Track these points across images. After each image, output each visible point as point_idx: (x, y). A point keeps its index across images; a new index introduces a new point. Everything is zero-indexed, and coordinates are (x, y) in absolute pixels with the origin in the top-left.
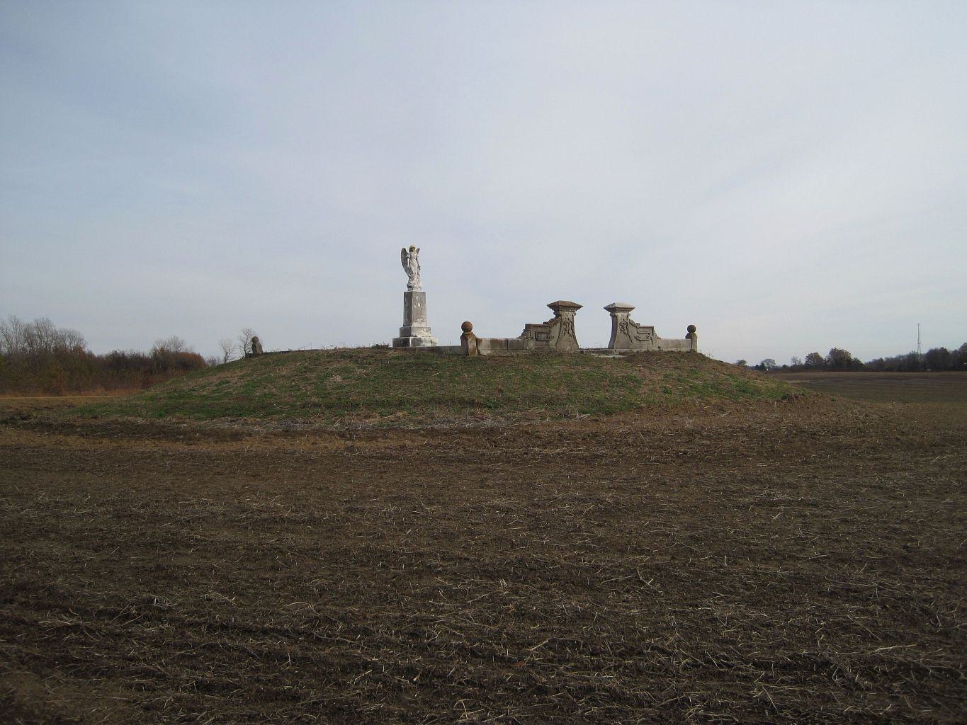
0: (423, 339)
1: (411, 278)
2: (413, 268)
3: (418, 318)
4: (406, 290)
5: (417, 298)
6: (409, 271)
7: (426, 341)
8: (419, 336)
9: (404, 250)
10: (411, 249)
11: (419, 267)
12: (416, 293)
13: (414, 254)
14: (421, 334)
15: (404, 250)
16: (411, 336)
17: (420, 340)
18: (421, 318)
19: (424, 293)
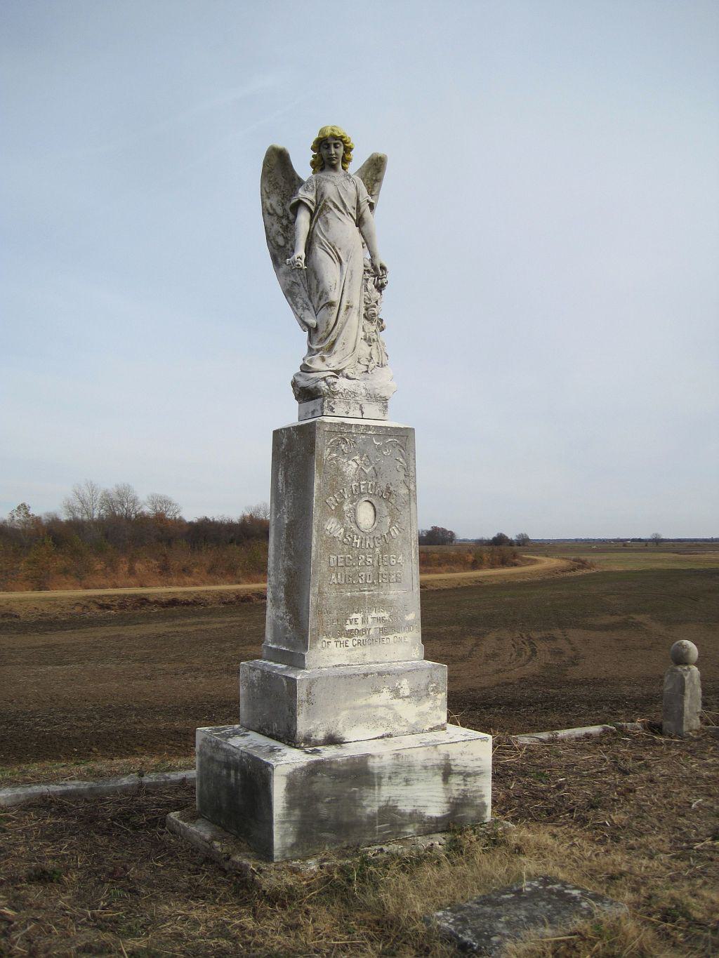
0: (382, 754)
1: (320, 337)
2: (330, 273)
3: (355, 604)
4: (289, 414)
5: (350, 468)
6: (303, 287)
7: (403, 771)
8: (361, 741)
9: (278, 162)
10: (329, 151)
11: (376, 273)
12: (341, 431)
13: (343, 185)
14: (375, 721)
15: (277, 165)
16: (289, 738)
17: (360, 774)
18: (384, 604)
19: (403, 438)
